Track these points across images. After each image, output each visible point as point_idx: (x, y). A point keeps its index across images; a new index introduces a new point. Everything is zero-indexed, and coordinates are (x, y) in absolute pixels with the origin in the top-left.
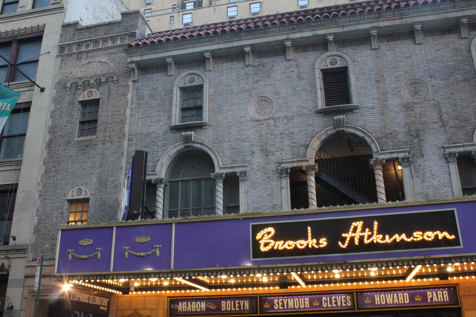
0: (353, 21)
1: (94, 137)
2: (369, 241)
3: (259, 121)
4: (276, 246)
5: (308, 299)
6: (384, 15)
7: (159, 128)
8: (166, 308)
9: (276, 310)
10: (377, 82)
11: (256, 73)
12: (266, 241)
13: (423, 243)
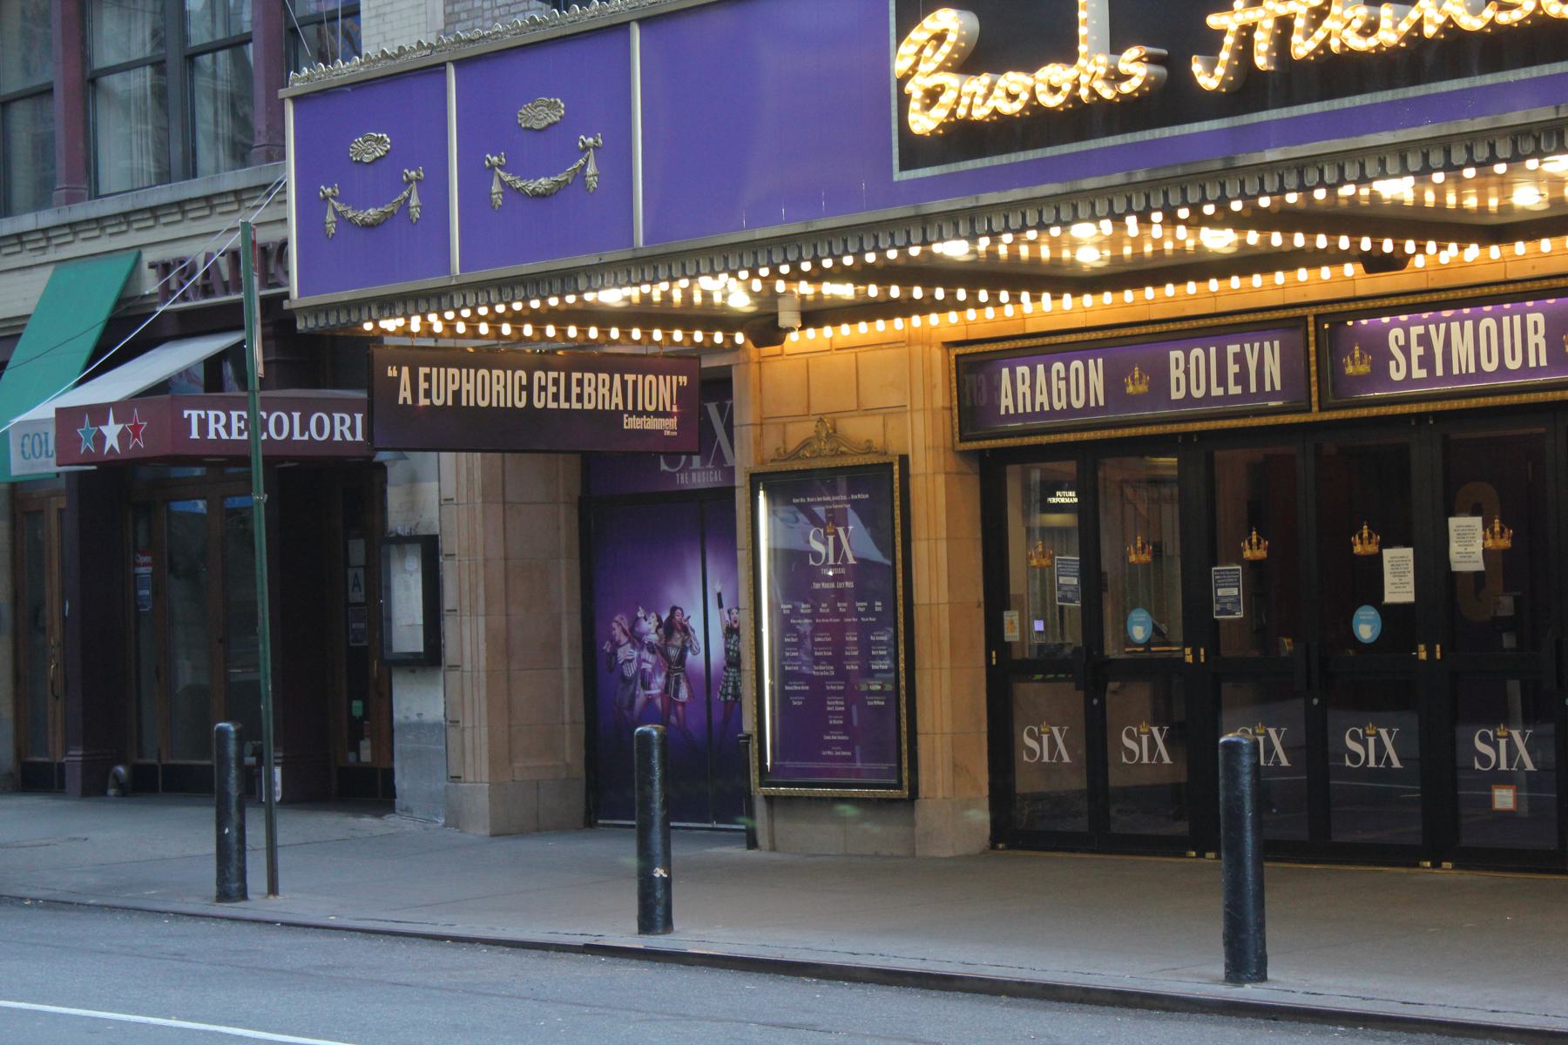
2: (1311, 45)
4: (965, 101)
5: (1539, 317)
9: (1400, 384)
12: (930, 83)
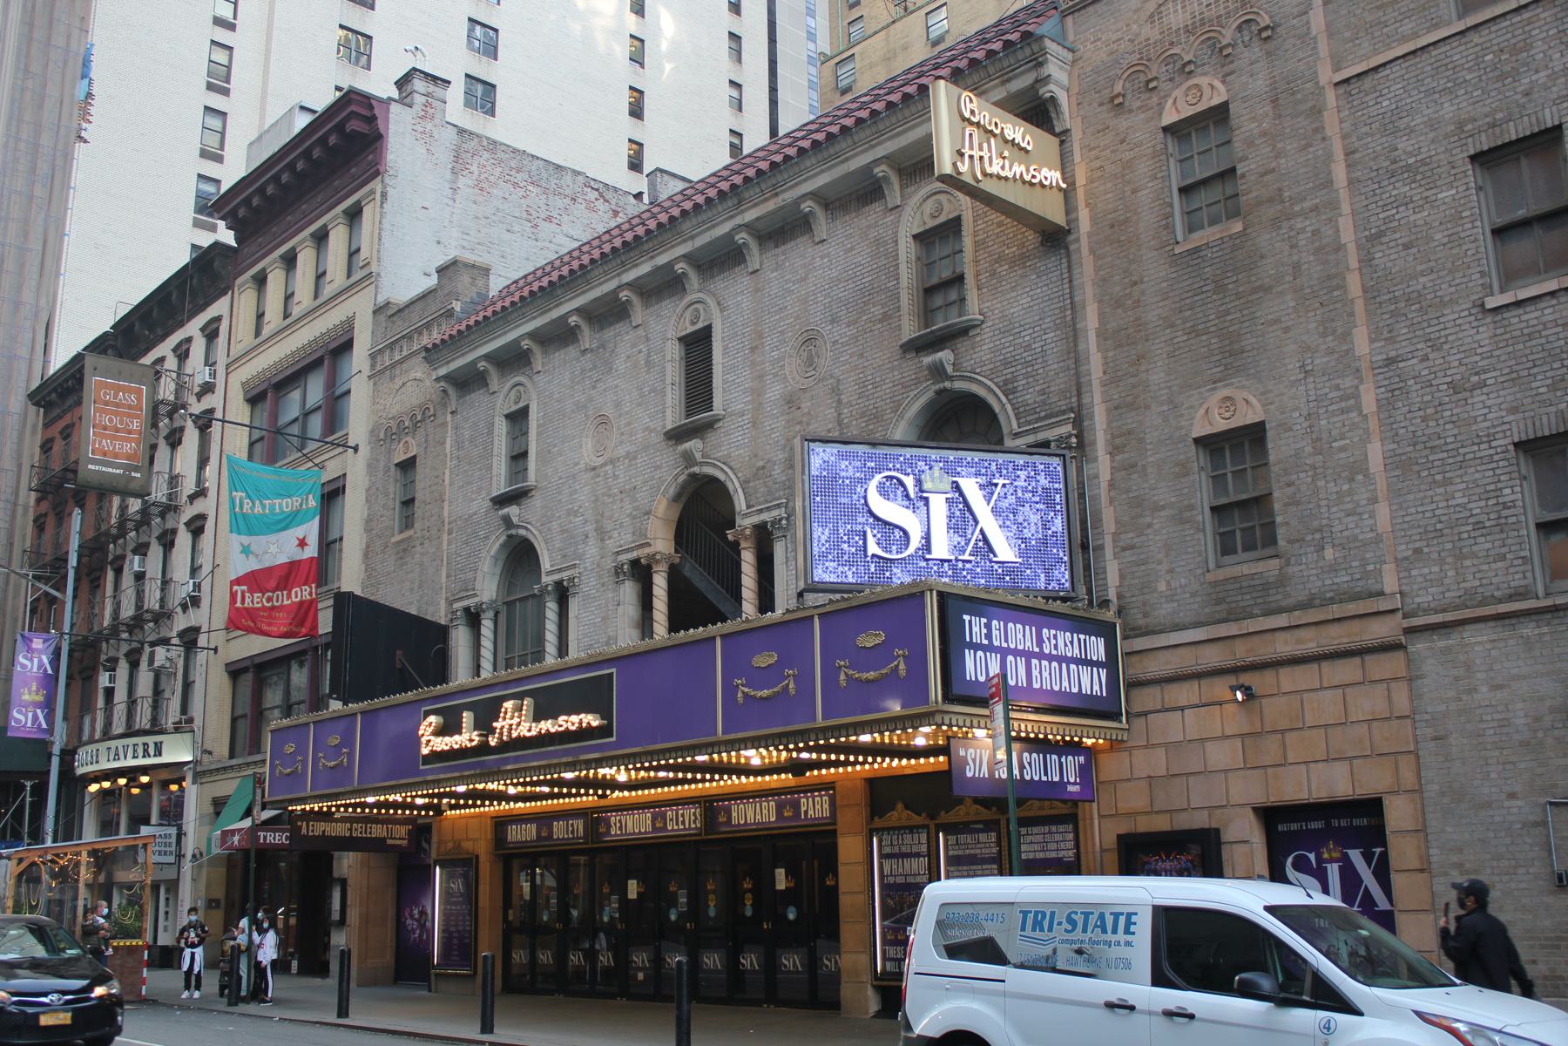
0: (704, 223)
1: (410, 532)
3: (594, 469)
6: (746, 195)
7: (481, 504)
8: (489, 836)
10: (753, 349)
11: (595, 367)
13: (566, 736)
